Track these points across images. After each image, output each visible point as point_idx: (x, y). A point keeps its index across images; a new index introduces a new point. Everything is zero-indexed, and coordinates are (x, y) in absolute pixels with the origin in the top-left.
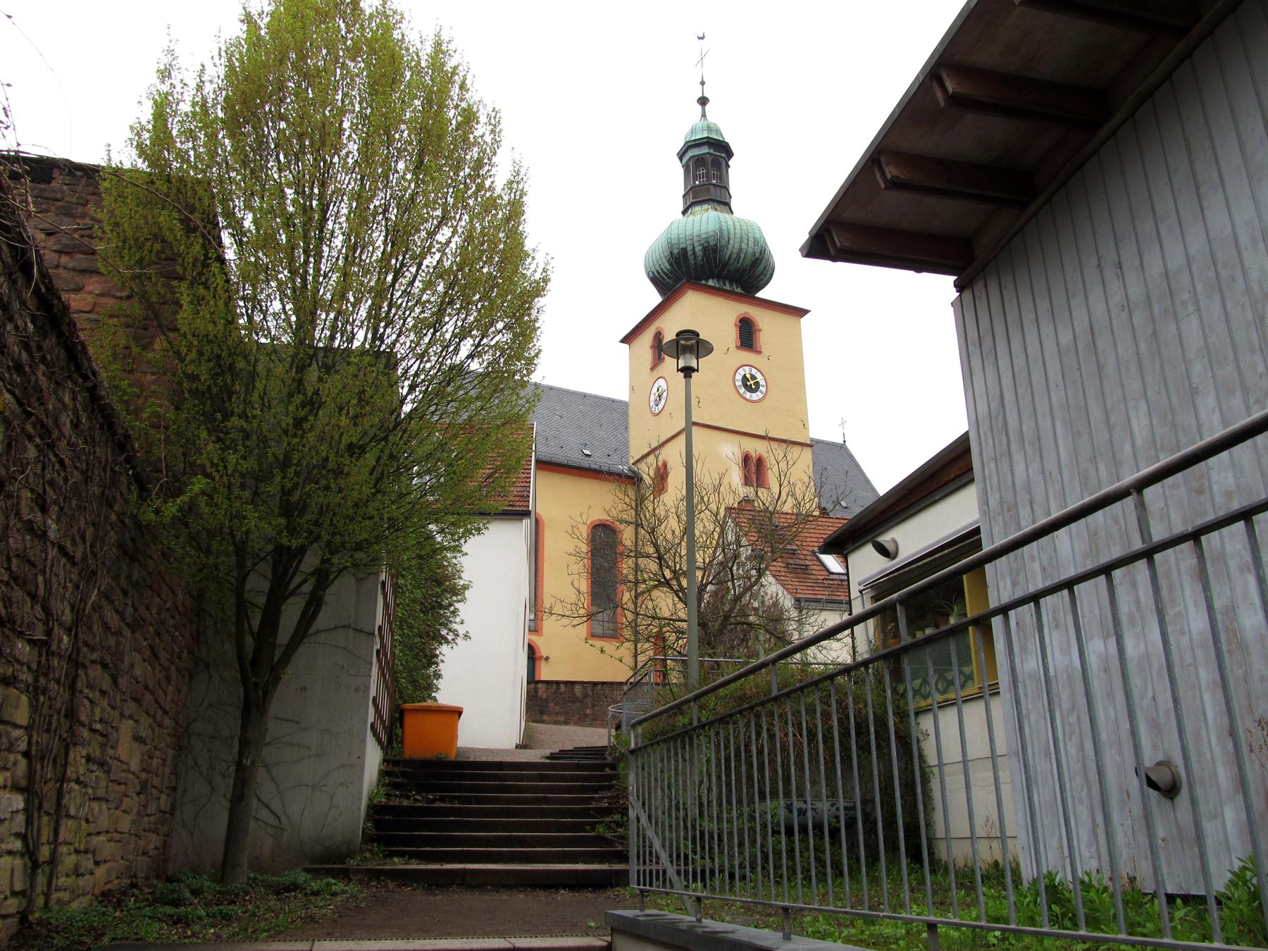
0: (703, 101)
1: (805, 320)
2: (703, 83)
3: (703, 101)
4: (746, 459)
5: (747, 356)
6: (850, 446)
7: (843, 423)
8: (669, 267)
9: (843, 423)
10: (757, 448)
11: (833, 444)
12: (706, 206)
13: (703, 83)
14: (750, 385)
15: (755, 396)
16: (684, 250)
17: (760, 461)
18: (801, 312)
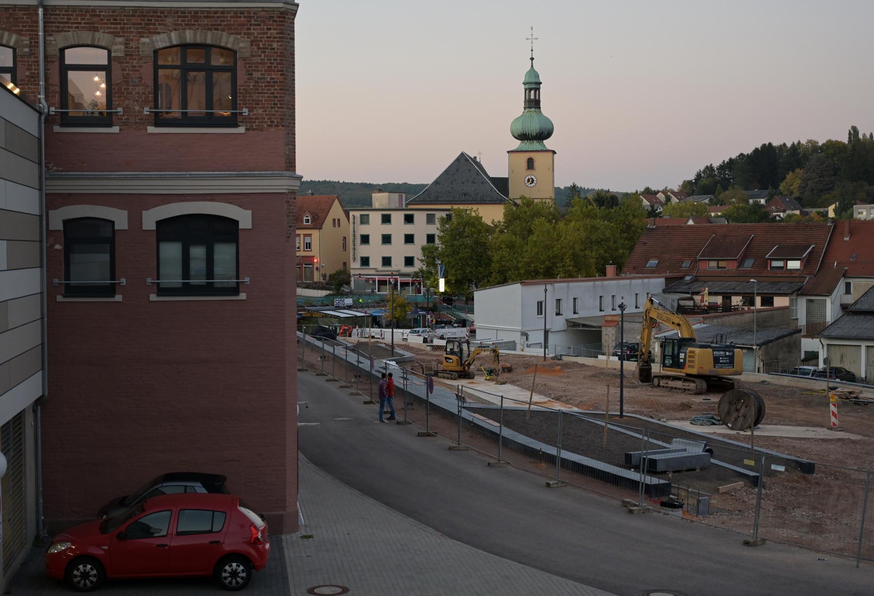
0: (532, 59)
2: (532, 50)
3: (532, 59)
8: (535, 135)
13: (532, 50)
16: (543, 132)
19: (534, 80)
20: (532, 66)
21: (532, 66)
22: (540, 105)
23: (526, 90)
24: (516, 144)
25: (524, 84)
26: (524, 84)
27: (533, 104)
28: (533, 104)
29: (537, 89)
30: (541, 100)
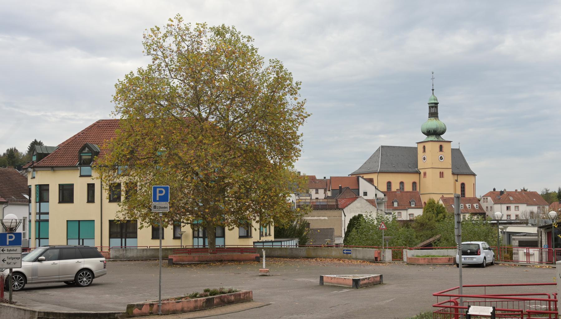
0: (433, 90)
1: (451, 143)
2: (433, 85)
3: (433, 90)
4: (440, 173)
5: (441, 153)
6: (460, 149)
7: (459, 143)
9: (459, 143)
10: (442, 170)
11: (456, 149)
12: (433, 118)
13: (433, 85)
14: (441, 158)
15: (442, 161)
16: (430, 131)
17: (442, 173)
18: (451, 142)
19: (433, 102)
20: (433, 94)
21: (433, 94)
22: (438, 115)
23: (430, 107)
24: (424, 137)
25: (429, 104)
26: (429, 104)
27: (434, 114)
28: (434, 114)
29: (436, 107)
30: (439, 112)
